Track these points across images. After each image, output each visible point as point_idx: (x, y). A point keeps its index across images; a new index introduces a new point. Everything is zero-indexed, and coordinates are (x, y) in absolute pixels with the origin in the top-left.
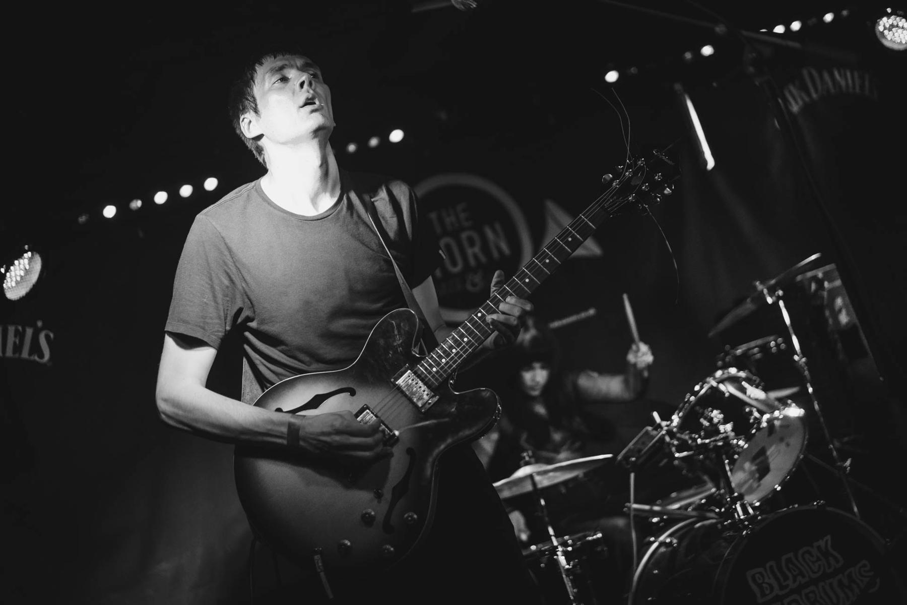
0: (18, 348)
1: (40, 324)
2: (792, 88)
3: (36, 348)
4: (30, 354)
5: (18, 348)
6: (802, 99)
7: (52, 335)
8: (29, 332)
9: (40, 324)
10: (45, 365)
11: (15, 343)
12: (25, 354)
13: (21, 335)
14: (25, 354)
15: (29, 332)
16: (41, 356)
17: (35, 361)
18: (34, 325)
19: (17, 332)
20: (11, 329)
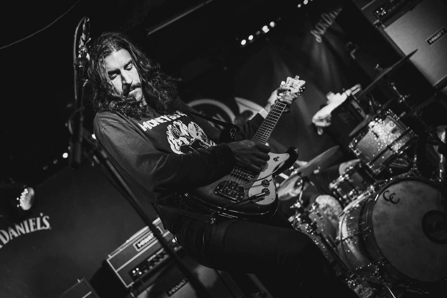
0: (35, 227)
1: (42, 214)
2: (319, 24)
3: (42, 224)
4: (41, 226)
5: (35, 227)
6: (325, 27)
7: (48, 217)
8: (38, 220)
9: (42, 214)
10: (48, 229)
11: (34, 226)
12: (39, 228)
13: (35, 221)
14: (39, 228)
15: (38, 220)
16: (46, 226)
17: (44, 230)
18: (39, 216)
19: (33, 221)
20: (31, 221)
